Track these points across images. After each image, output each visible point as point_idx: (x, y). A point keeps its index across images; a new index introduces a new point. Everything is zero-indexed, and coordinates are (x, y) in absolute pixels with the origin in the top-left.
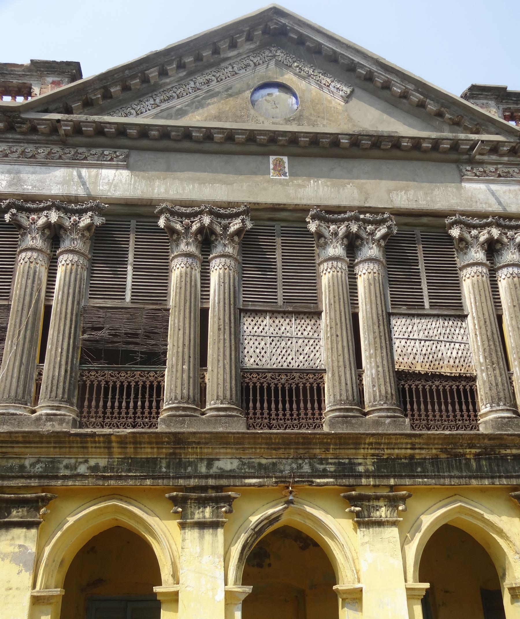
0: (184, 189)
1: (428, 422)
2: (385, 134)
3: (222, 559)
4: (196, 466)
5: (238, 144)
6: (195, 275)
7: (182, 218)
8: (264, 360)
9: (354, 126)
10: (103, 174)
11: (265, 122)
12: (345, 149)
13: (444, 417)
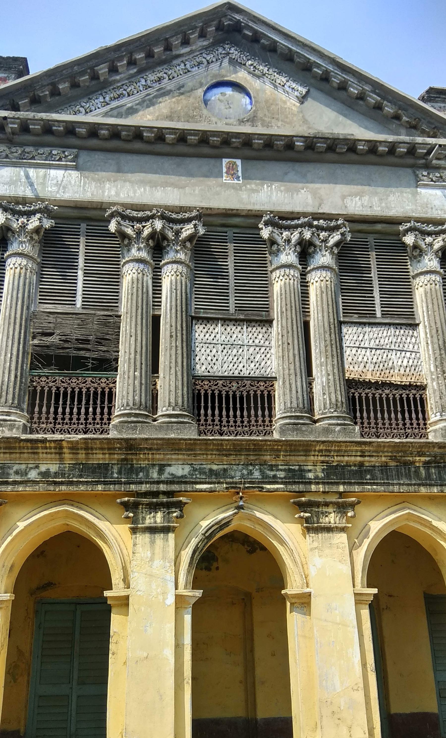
0: (135, 192)
1: (377, 430)
2: (341, 137)
3: (173, 564)
4: (148, 472)
5: (190, 145)
6: (147, 281)
7: (133, 222)
8: (215, 367)
9: (309, 128)
10: (51, 175)
11: (219, 122)
12: (299, 152)
13: (394, 426)
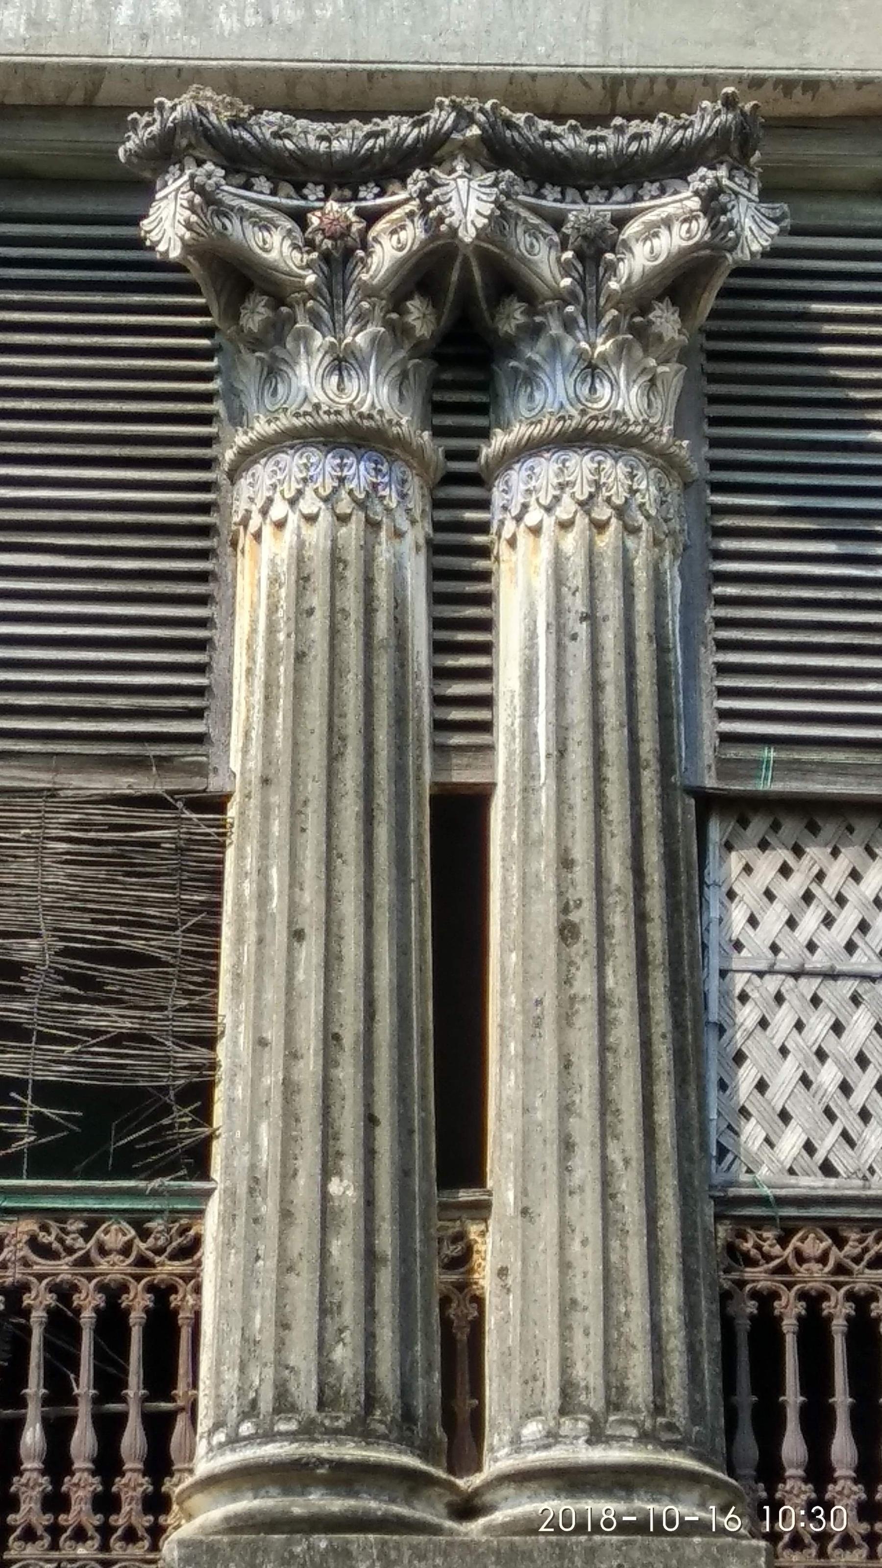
6: (397, 570)
7: (299, 188)
